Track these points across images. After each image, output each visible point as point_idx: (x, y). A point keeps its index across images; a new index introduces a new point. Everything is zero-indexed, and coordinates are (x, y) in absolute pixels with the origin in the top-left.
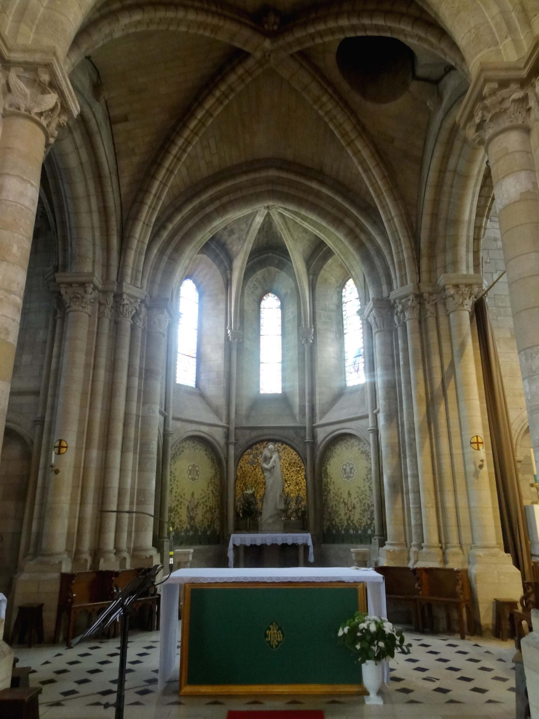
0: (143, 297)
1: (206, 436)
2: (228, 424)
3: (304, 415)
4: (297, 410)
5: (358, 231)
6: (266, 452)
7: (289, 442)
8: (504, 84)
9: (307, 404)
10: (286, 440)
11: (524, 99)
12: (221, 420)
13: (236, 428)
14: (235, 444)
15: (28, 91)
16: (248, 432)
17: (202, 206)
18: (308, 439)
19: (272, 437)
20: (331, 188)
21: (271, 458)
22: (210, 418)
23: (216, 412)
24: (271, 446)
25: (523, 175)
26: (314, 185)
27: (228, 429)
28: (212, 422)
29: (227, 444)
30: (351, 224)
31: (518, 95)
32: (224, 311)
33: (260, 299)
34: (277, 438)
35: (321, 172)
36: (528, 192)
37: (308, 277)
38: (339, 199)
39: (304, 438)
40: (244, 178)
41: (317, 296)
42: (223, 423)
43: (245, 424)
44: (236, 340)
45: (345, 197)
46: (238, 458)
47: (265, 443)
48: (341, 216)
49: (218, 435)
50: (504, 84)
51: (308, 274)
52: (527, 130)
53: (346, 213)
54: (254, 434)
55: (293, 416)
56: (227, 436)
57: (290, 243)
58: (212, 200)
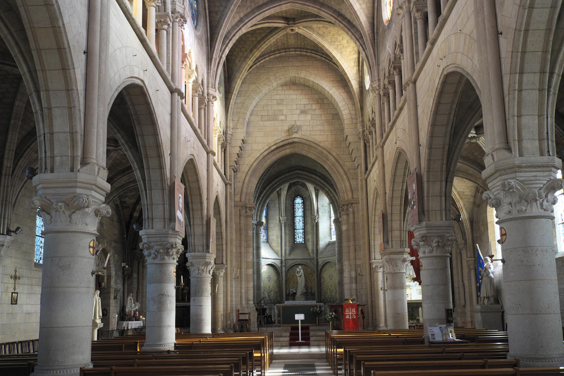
0: (255, 223)
1: (273, 264)
2: (282, 258)
3: (314, 253)
4: (310, 251)
5: (329, 192)
6: (298, 270)
7: (308, 265)
8: (343, 205)
9: (315, 249)
10: (306, 264)
11: (348, 208)
12: (279, 256)
13: (285, 260)
14: (285, 266)
15: (250, 212)
16: (290, 261)
17: (273, 185)
18: (315, 263)
19: (300, 263)
20: (320, 177)
21: (300, 272)
22: (275, 256)
23: (277, 253)
24: (300, 267)
25: (346, 225)
26: (313, 176)
27: (282, 260)
28: (276, 258)
29: (281, 266)
30: (328, 190)
31: (346, 208)
32: (278, 208)
33: (294, 199)
34: (302, 263)
35: (315, 171)
36: (347, 229)
37: (315, 191)
38: (322, 181)
39: (313, 263)
40: (288, 174)
41: (319, 198)
42: (280, 258)
43: (288, 258)
44: (284, 221)
45: (324, 180)
46: (287, 272)
47: (297, 266)
48: (323, 186)
49: (278, 263)
50: (343, 205)
51: (315, 190)
52: (348, 215)
53: (326, 186)
54: (293, 262)
55: (309, 254)
56: (281, 263)
57: (319, 39)
58: (276, 183)
